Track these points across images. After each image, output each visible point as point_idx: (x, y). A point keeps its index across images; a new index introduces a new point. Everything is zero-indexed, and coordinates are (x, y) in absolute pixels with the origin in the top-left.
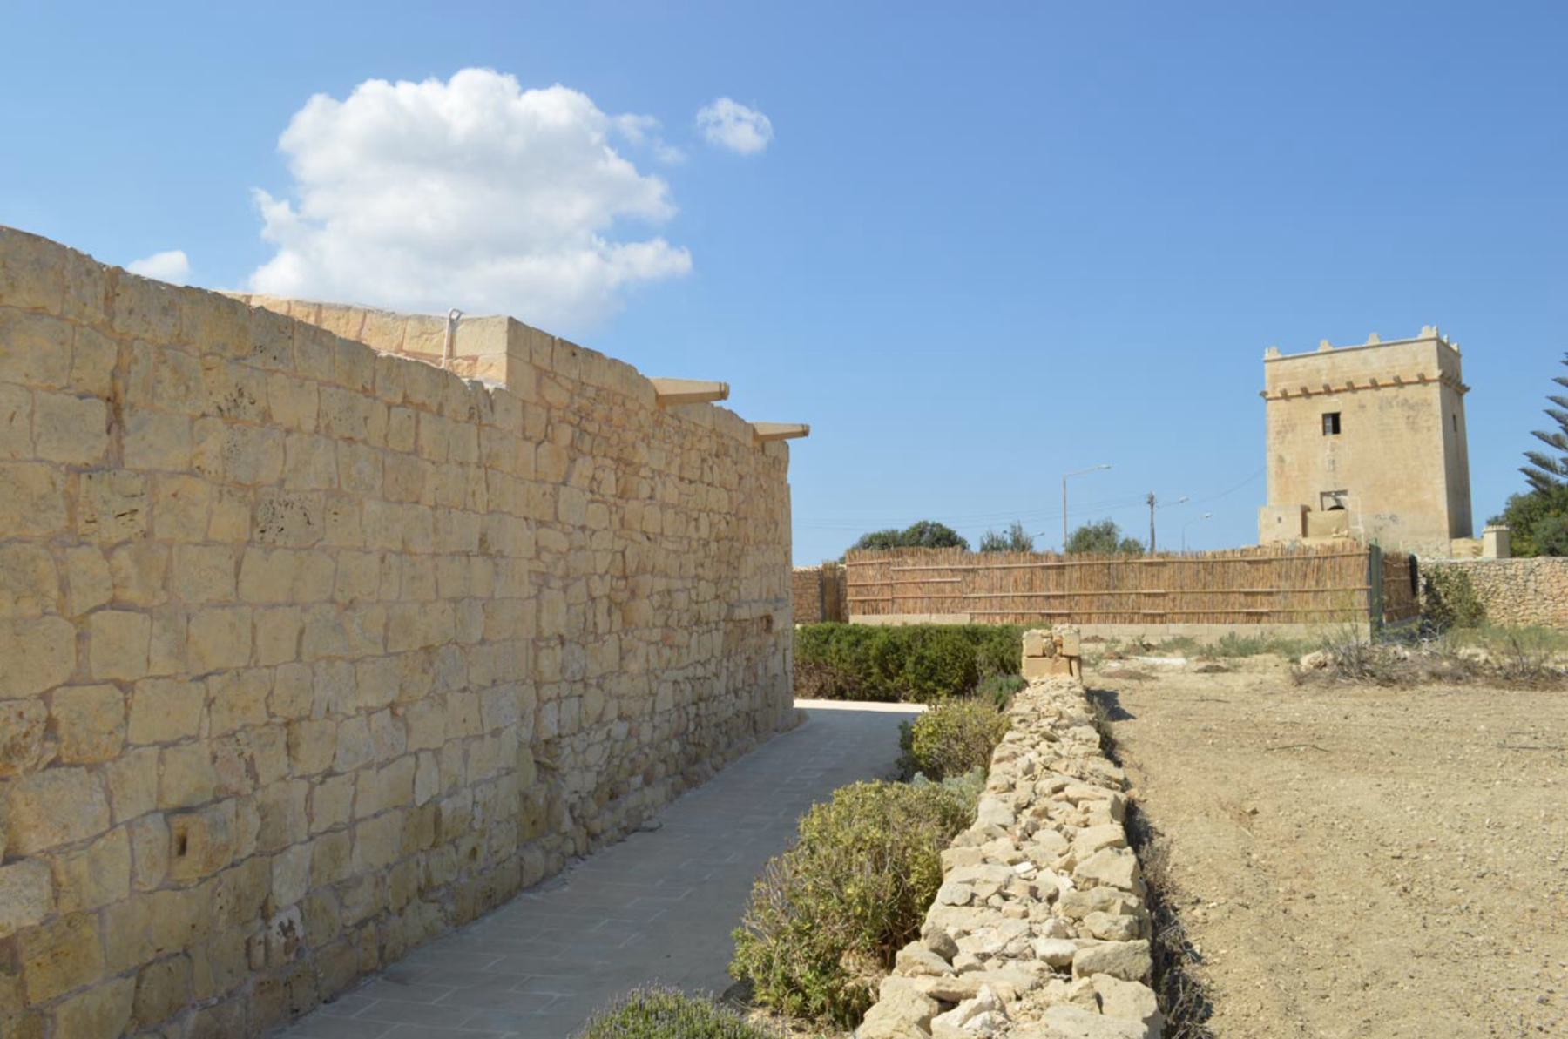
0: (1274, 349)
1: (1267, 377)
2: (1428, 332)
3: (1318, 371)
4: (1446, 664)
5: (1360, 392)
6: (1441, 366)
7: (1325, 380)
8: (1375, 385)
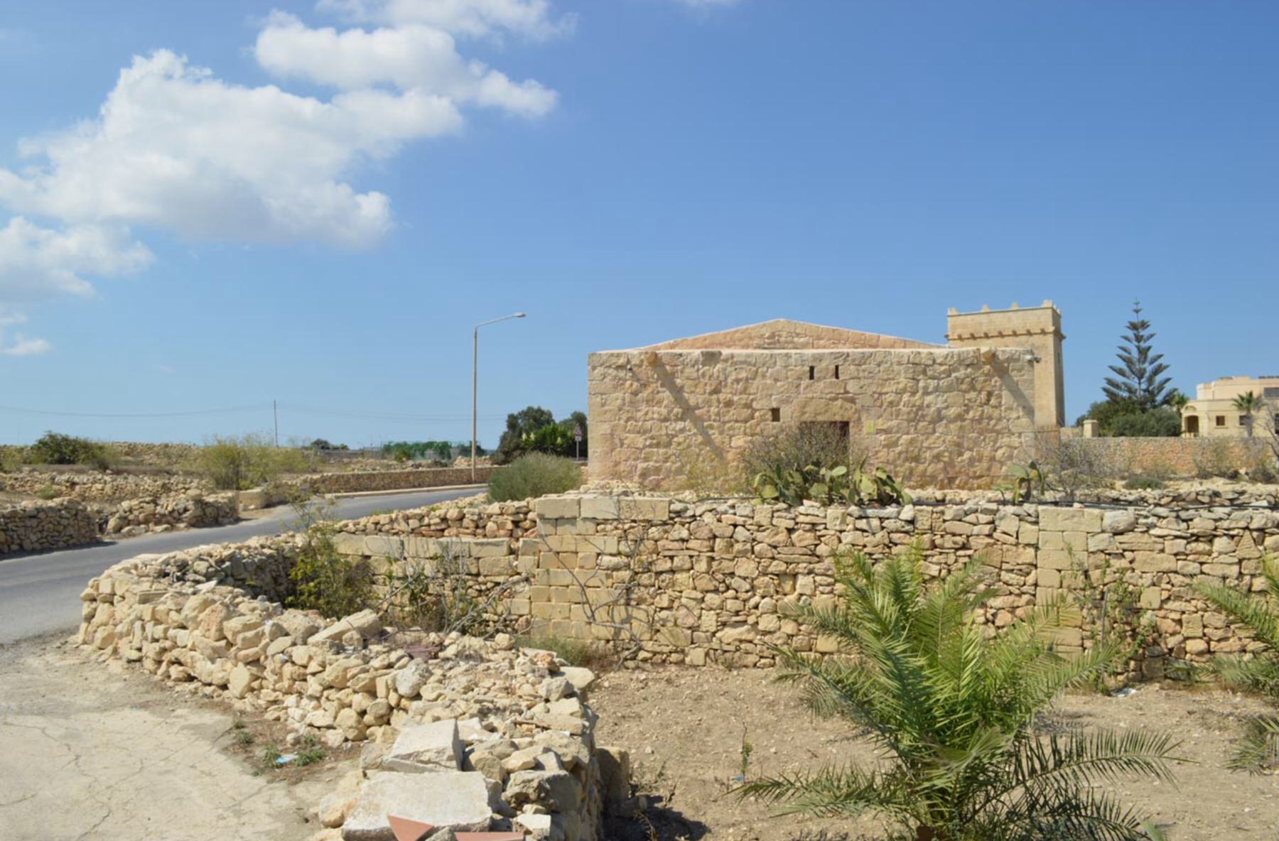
0: (954, 309)
1: (949, 325)
2: (1047, 303)
3: (981, 324)
4: (1126, 474)
5: (1006, 338)
6: (1054, 325)
7: (984, 329)
8: (1015, 334)
